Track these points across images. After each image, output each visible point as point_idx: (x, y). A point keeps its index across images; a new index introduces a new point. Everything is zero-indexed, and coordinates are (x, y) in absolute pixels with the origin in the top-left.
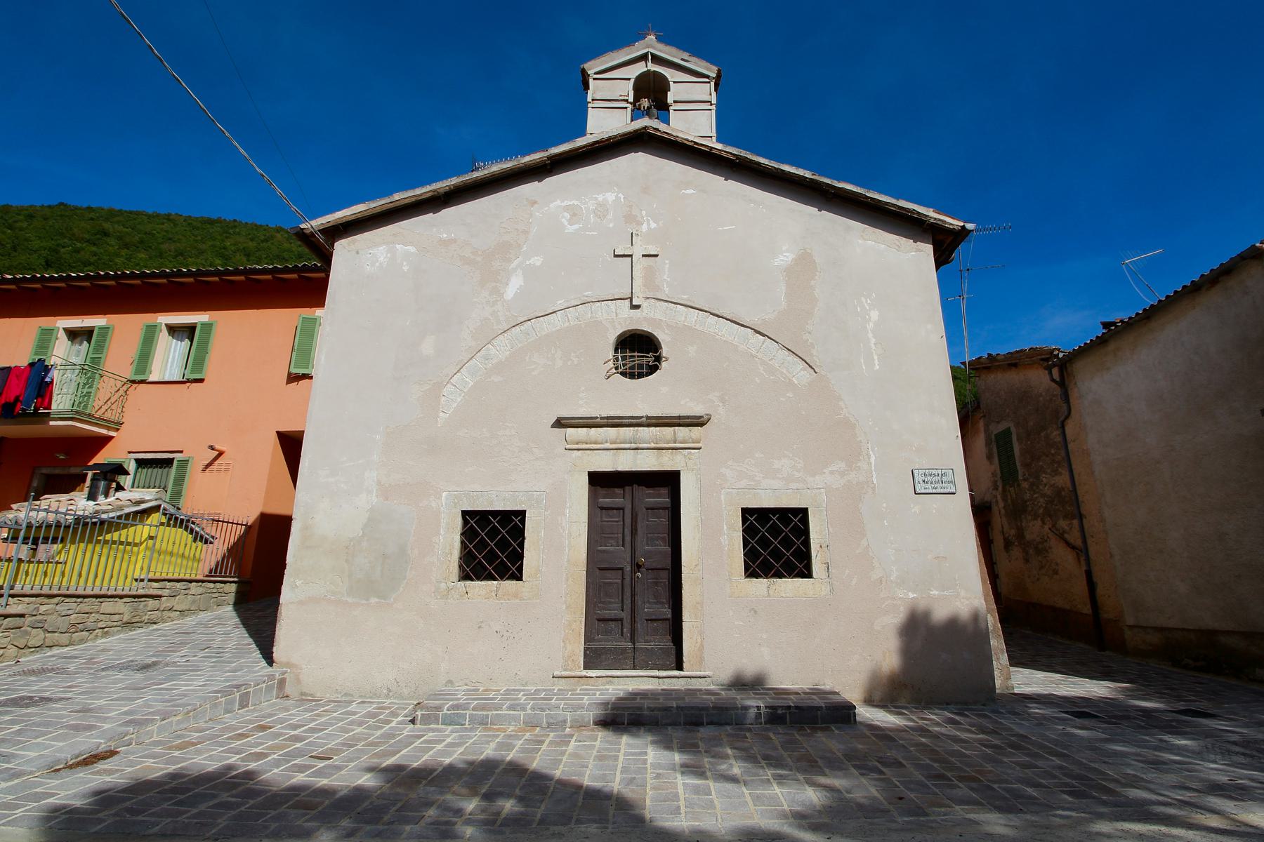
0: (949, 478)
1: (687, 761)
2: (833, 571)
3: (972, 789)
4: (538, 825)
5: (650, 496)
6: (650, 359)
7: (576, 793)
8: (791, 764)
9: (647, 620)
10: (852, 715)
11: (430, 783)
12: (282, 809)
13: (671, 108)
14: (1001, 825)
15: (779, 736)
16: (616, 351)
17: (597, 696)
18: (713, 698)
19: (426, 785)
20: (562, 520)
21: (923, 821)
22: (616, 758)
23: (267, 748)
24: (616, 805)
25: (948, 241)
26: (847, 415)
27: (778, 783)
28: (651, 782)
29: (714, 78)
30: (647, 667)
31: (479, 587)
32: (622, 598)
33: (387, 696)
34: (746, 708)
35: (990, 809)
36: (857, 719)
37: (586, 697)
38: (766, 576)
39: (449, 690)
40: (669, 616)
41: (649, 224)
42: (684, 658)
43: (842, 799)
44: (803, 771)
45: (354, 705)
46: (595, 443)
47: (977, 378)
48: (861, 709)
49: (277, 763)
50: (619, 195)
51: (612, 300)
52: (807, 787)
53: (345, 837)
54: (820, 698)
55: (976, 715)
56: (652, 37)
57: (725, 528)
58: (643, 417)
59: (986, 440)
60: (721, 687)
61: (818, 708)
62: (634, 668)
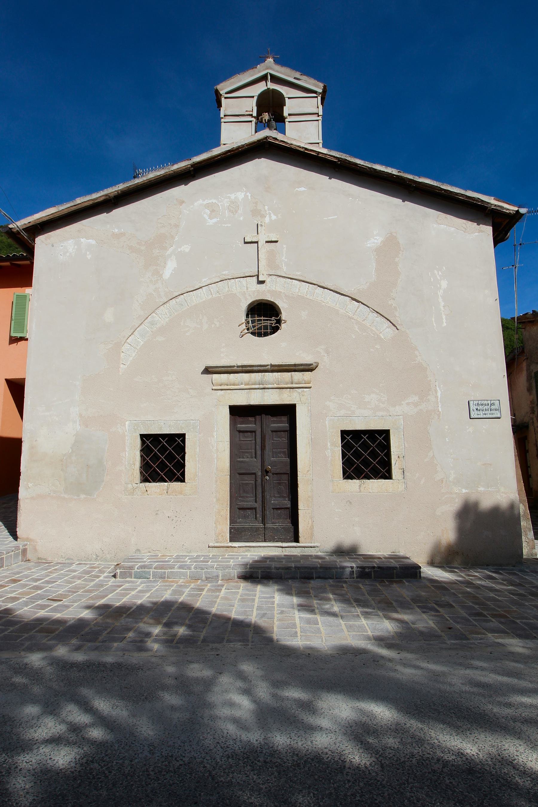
0: (496, 407)
1: (302, 603)
2: (407, 474)
3: (501, 623)
4: (202, 642)
5: (274, 422)
6: (273, 322)
7: (226, 623)
8: (374, 605)
9: (273, 509)
10: (418, 572)
11: (129, 616)
12: (32, 633)
13: (287, 120)
14: (520, 646)
15: (366, 586)
16: (247, 316)
17: (240, 559)
18: (320, 561)
19: (126, 617)
20: (211, 440)
21: (465, 643)
22: (253, 600)
23: (19, 594)
24: (254, 631)
25: (505, 223)
26: (421, 361)
27: (365, 617)
28: (277, 616)
29: (320, 93)
30: (274, 540)
31: (155, 487)
32: (256, 494)
33: (96, 559)
34: (344, 568)
35: (513, 636)
36: (422, 575)
37: (232, 560)
38: (359, 478)
39: (138, 556)
40: (289, 506)
41: (270, 217)
42: (300, 534)
43: (409, 628)
44: (383, 610)
45: (74, 565)
46: (234, 385)
47: (523, 330)
48: (425, 569)
49: (26, 604)
50: (247, 194)
51: (243, 277)
52: (385, 620)
53: (75, 650)
54: (395, 561)
55: (507, 573)
56: (270, 60)
57: (329, 444)
58: (268, 365)
59: (527, 377)
60: (328, 554)
61: (394, 568)
62: (265, 541)
